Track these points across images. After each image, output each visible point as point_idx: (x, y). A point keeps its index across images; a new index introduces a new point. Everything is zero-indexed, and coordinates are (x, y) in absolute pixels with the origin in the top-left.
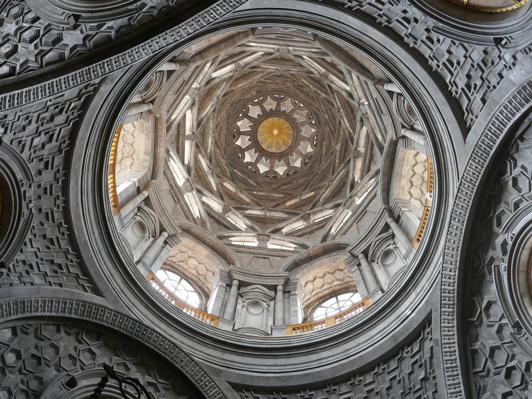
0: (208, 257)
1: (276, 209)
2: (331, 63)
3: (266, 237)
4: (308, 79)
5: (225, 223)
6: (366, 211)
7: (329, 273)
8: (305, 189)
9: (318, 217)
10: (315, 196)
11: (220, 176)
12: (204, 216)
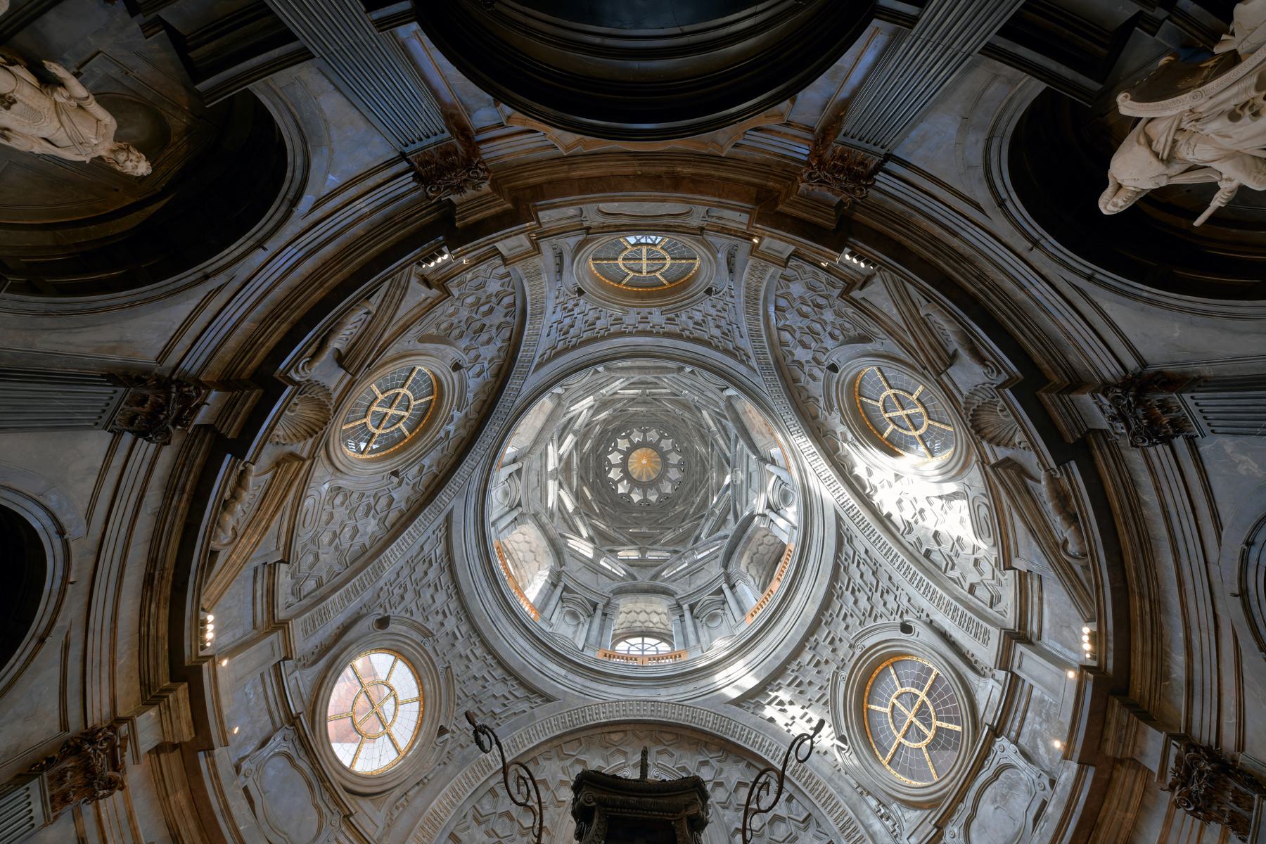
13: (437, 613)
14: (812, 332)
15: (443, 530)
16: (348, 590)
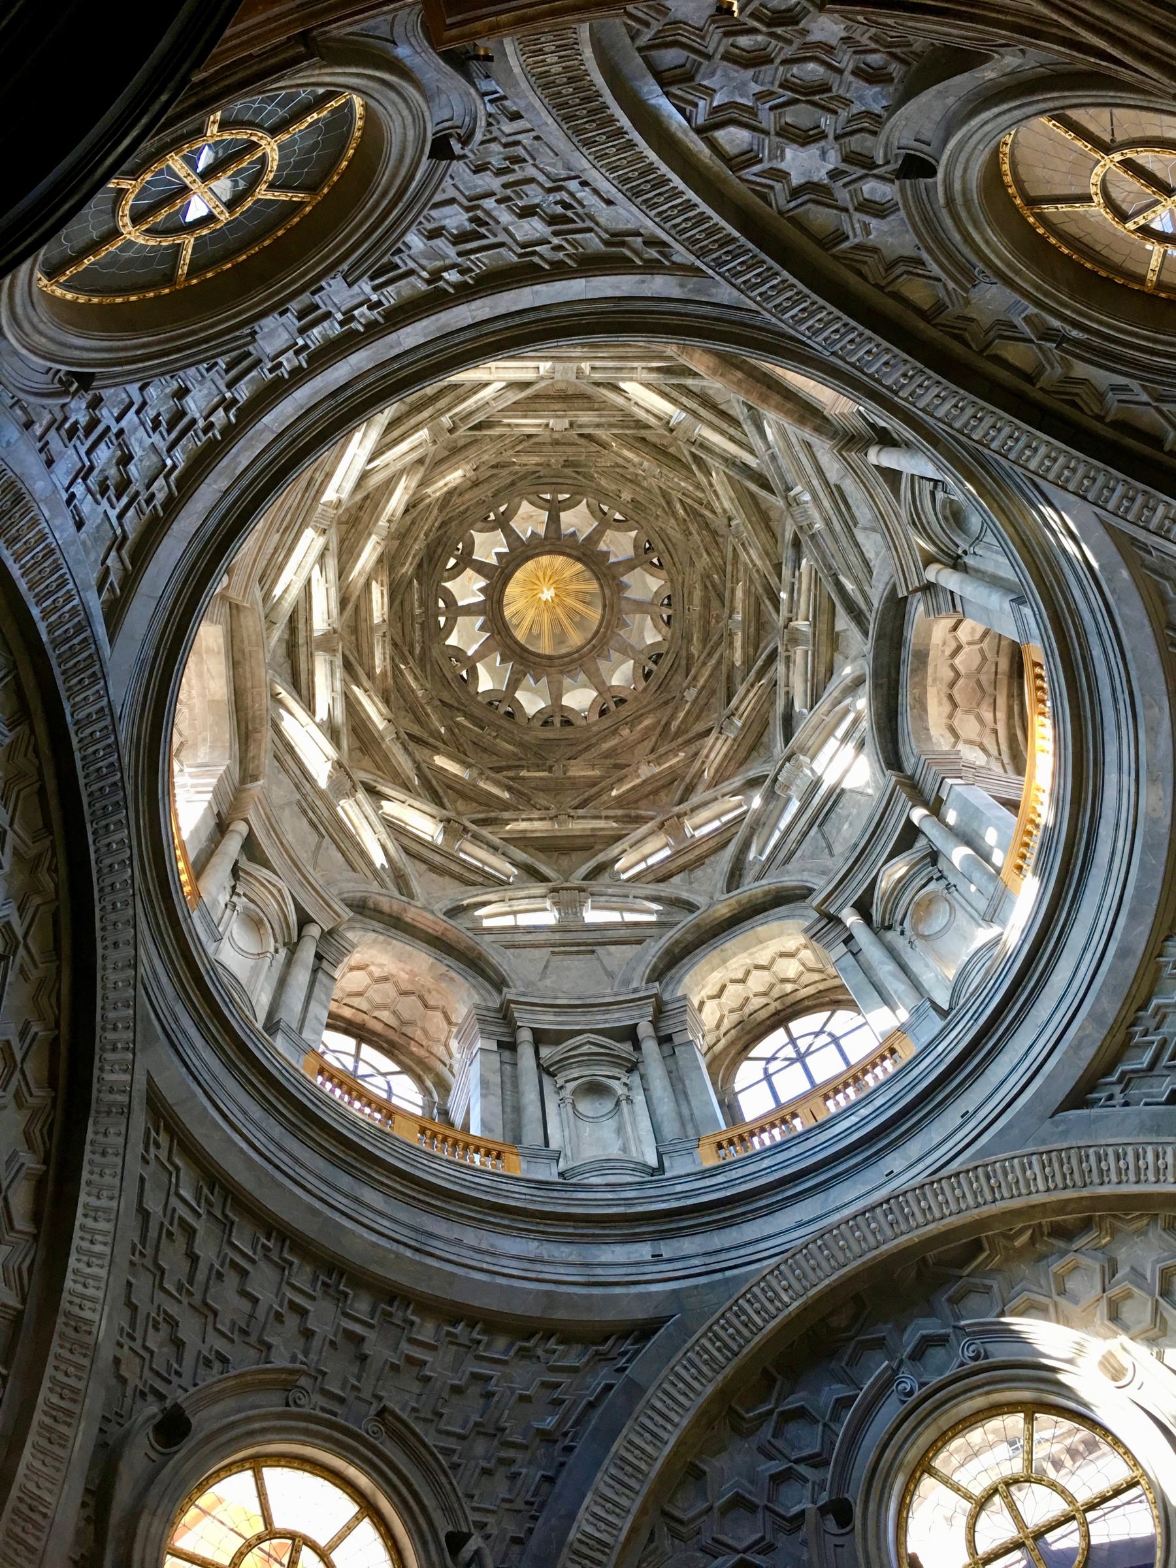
0: (212, 704)
1: (412, 746)
2: (838, 634)
3: (349, 784)
4: (752, 599)
5: (303, 666)
6: (593, 952)
7: (396, 984)
8: (498, 770)
9: (474, 854)
10: (505, 806)
11: (388, 561)
12: (287, 606)
13: (279, 1317)
14: (811, 92)
15: (163, 1139)
16: (42, 1425)
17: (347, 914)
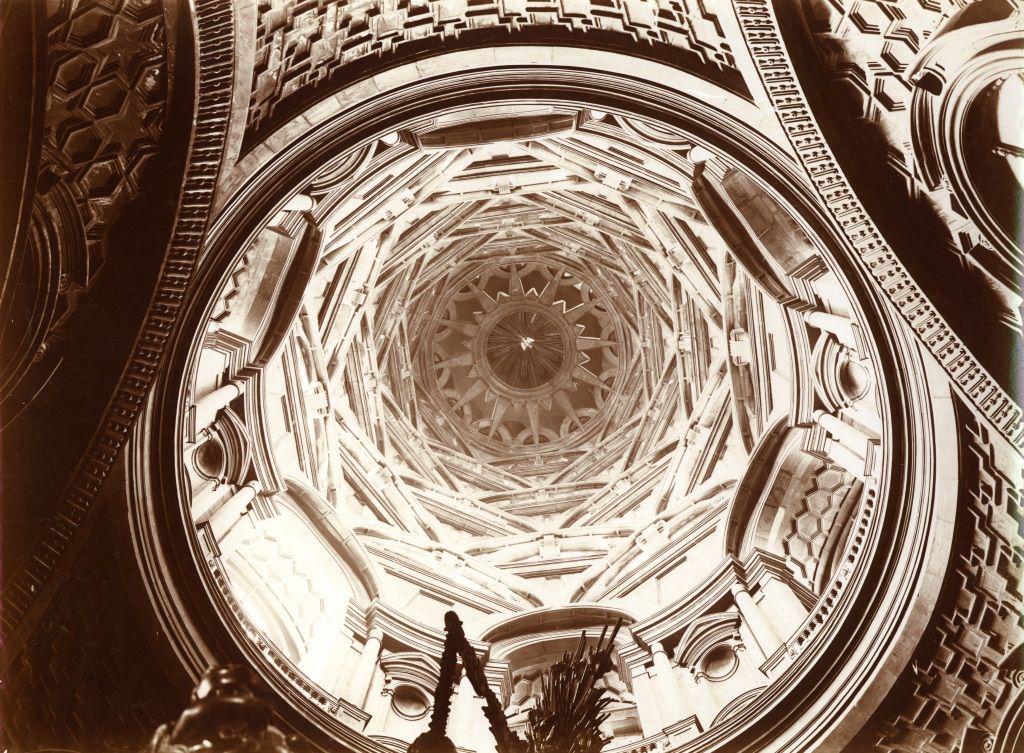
17: (283, 489)
